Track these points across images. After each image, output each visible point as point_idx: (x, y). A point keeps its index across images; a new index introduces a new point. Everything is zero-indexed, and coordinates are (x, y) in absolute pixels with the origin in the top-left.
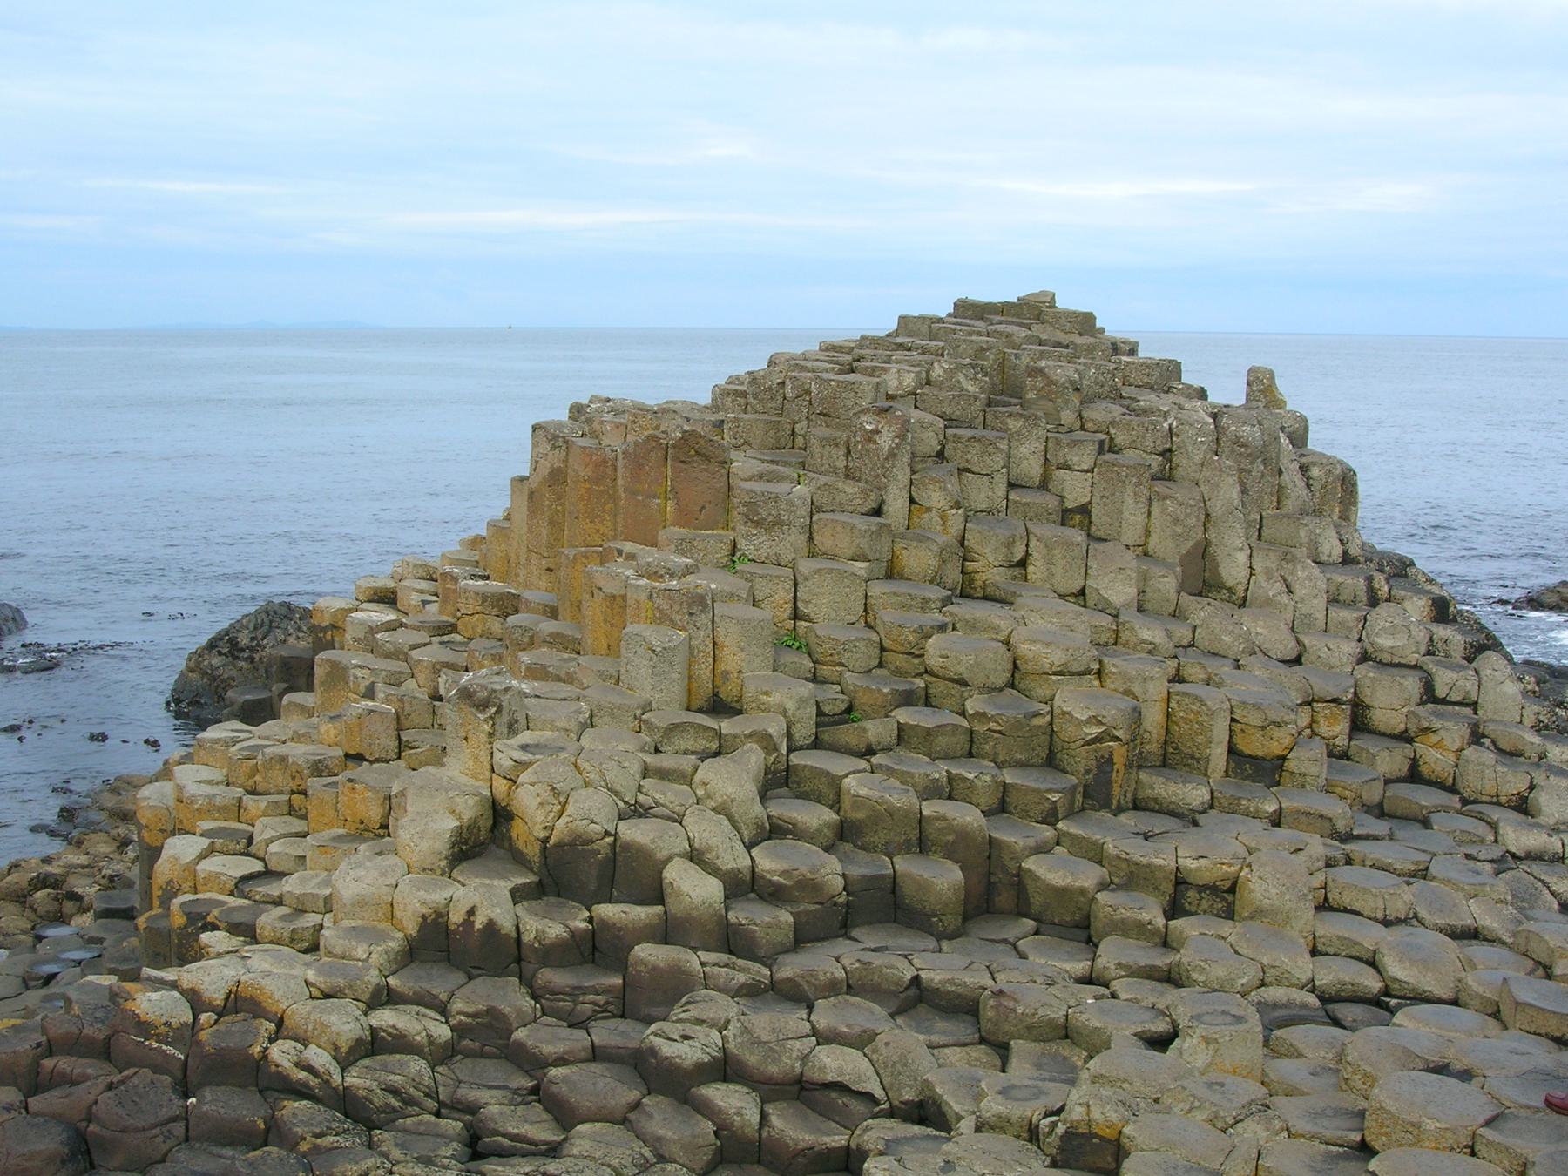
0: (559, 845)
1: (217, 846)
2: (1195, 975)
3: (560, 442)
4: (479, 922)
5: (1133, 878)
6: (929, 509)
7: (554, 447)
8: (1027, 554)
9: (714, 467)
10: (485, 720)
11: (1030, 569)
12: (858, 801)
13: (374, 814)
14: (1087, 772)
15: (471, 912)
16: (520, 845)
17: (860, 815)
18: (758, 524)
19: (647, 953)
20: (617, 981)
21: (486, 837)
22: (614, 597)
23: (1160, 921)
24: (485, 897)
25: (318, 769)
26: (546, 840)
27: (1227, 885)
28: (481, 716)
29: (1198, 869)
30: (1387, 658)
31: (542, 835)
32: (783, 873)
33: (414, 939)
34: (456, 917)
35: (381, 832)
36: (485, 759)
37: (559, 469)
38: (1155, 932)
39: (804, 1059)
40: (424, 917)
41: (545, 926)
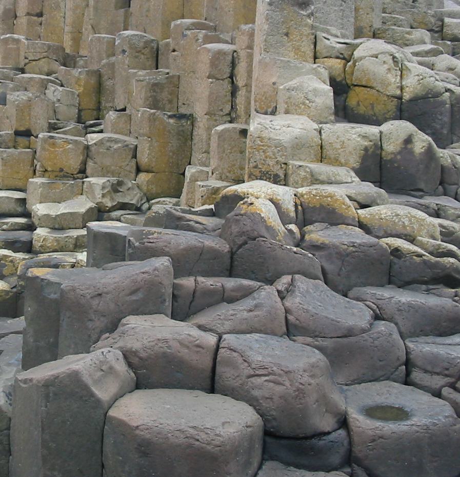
15: (408, 141)
26: (400, 98)
31: (398, 92)
33: (360, 168)
34: (390, 147)
35: (80, 175)
37: (9, 10)
40: (366, 149)
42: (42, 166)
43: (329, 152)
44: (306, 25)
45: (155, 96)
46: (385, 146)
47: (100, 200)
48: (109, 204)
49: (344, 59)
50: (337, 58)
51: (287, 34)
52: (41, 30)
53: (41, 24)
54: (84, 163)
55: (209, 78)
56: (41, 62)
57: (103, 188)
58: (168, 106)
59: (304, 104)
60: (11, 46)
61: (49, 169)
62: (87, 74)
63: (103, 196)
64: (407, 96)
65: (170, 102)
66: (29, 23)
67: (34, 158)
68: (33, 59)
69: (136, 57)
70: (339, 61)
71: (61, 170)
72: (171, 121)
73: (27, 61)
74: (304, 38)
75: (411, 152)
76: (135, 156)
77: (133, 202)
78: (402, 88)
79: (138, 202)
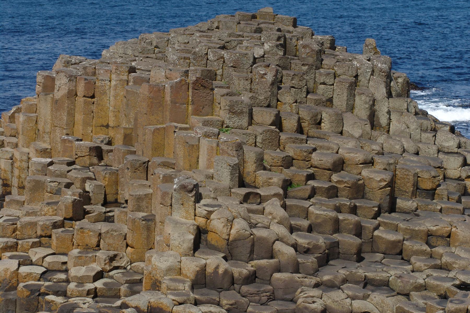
0: (235, 240)
1: (21, 262)
2: (454, 266)
3: (73, 78)
4: (221, 271)
5: (413, 235)
6: (285, 104)
7: (70, 80)
8: (321, 119)
9: (208, 91)
10: (192, 197)
11: (323, 124)
12: (318, 216)
13: (94, 241)
14: (381, 199)
15: (217, 267)
16: (213, 243)
17: (319, 221)
18: (234, 113)
19: (277, 275)
20: (270, 287)
21: (200, 240)
22: (193, 145)
23: (429, 249)
24: (213, 261)
25: (55, 226)
26: (228, 240)
27: (446, 235)
28: (190, 195)
29: (437, 230)
30: (446, 150)
31: (227, 237)
32: (308, 244)
34: (209, 270)
35: (97, 248)
36: (192, 212)
37: (72, 90)
38: (428, 254)
39: (351, 305)
40: (198, 272)
41: (241, 270)
42: (77, 243)
43: (184, 271)
44: (191, 201)
45: (139, 205)
46: (207, 270)
47: (103, 267)
48: (108, 269)
49: (207, 218)
50: (203, 217)
51: (182, 204)
52: (94, 108)
53: (93, 103)
54: (99, 241)
55: (161, 204)
56: (85, 158)
57: (105, 260)
58: (146, 210)
59: (178, 246)
60: (68, 145)
61: (81, 244)
62: (110, 174)
63: (105, 264)
64: (231, 239)
65: (147, 207)
66: (85, 102)
67: (73, 238)
68: (81, 155)
69: (135, 172)
70: (204, 219)
71: (87, 245)
72: (144, 222)
73: (77, 156)
74: (190, 207)
75: (217, 272)
76: (125, 239)
77: (123, 265)
78: (229, 235)
79: (125, 265)
